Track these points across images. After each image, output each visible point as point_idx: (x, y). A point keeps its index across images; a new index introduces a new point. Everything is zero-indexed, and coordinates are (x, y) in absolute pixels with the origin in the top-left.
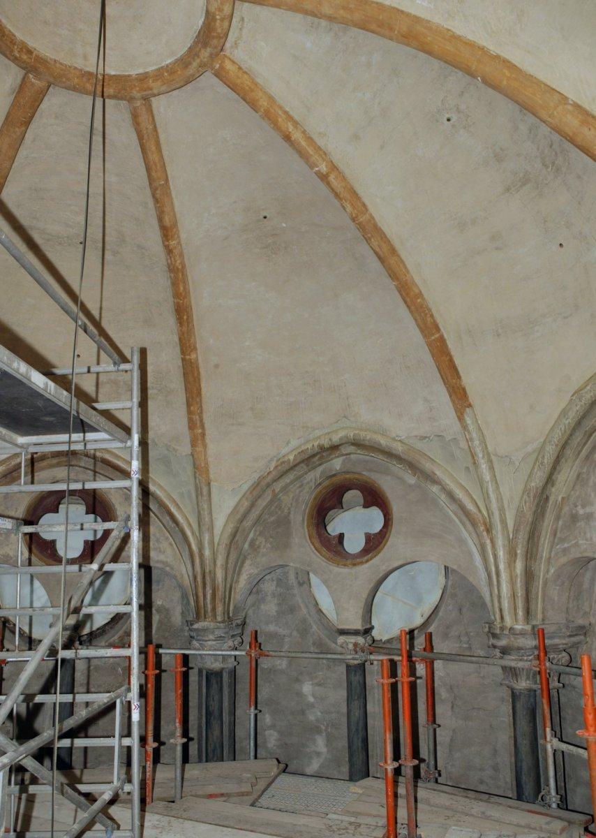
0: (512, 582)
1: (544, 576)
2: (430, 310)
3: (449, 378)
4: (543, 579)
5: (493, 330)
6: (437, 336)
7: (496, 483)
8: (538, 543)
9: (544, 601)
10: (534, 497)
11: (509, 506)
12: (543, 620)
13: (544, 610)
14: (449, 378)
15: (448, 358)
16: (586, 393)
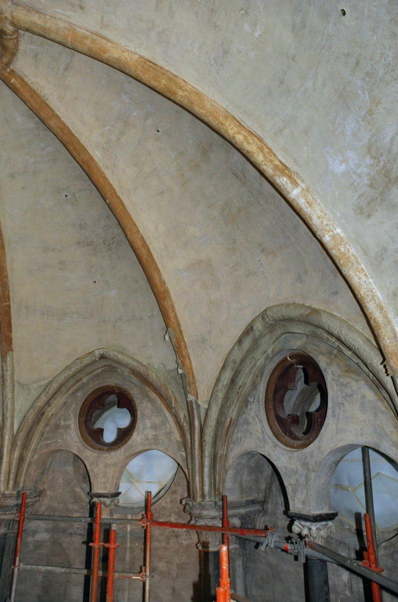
0: (10, 464)
1: (29, 460)
2: (8, 287)
3: (6, 330)
4: (29, 461)
5: (41, 310)
6: (8, 303)
7: (14, 400)
8: (31, 439)
9: (26, 475)
10: (37, 412)
11: (18, 415)
12: (23, 487)
13: (25, 480)
14: (6, 330)
15: (9, 319)
16: (85, 360)
